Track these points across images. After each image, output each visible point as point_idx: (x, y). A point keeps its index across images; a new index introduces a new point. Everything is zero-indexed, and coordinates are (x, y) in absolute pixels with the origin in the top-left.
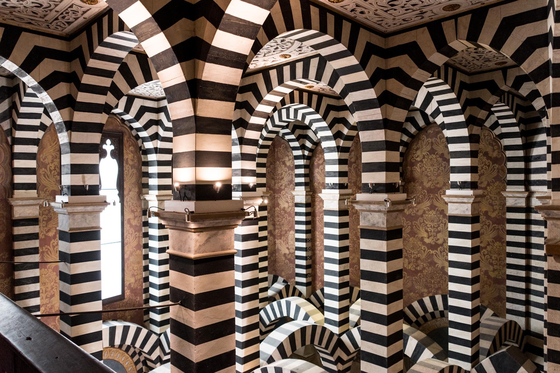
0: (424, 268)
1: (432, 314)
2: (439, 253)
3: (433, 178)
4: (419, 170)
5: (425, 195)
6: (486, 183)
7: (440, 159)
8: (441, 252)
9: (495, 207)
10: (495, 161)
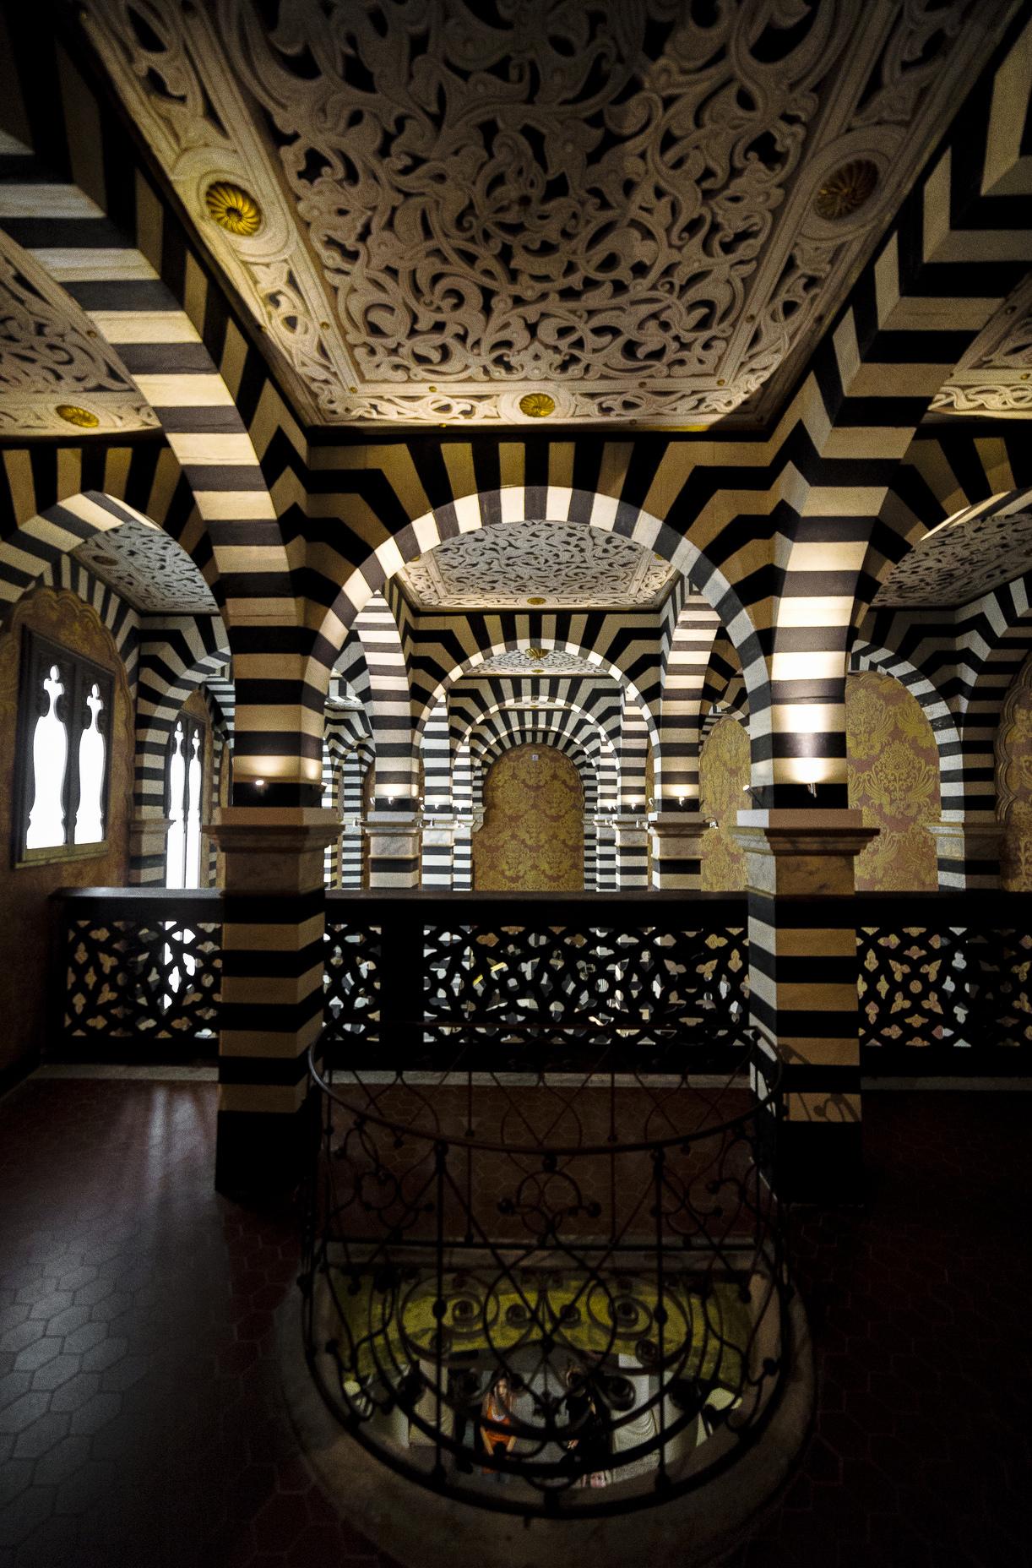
10: (572, 789)
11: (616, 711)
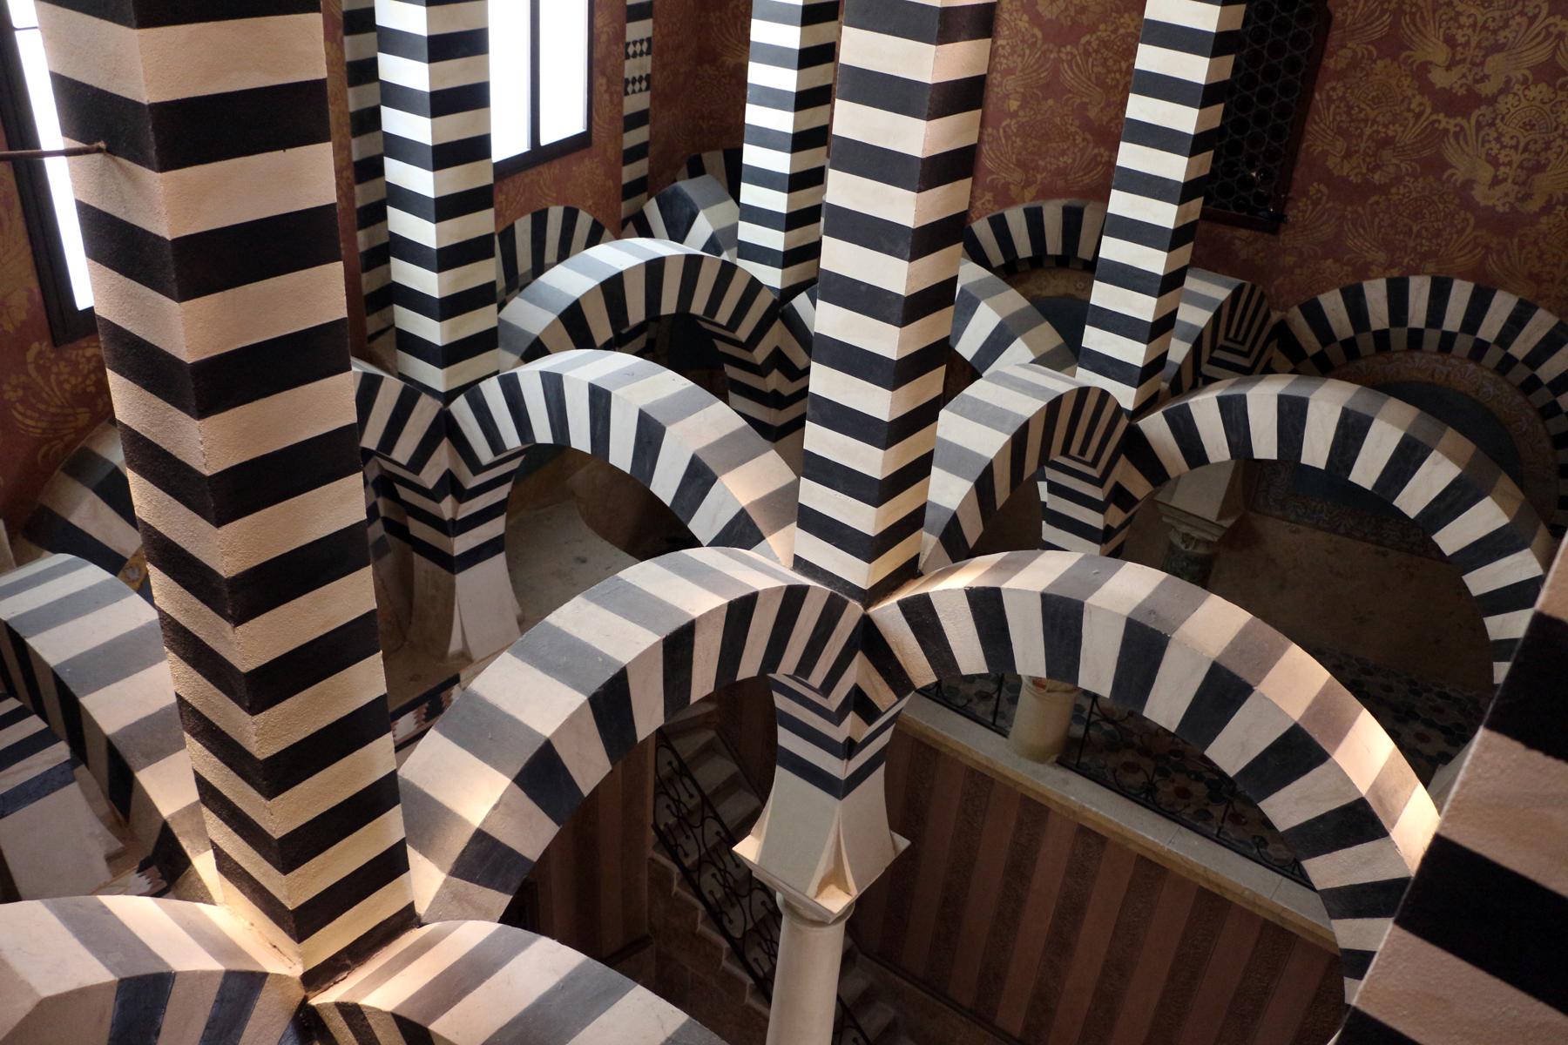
0: (1398, 180)
1: (1382, 338)
8: (1479, 126)
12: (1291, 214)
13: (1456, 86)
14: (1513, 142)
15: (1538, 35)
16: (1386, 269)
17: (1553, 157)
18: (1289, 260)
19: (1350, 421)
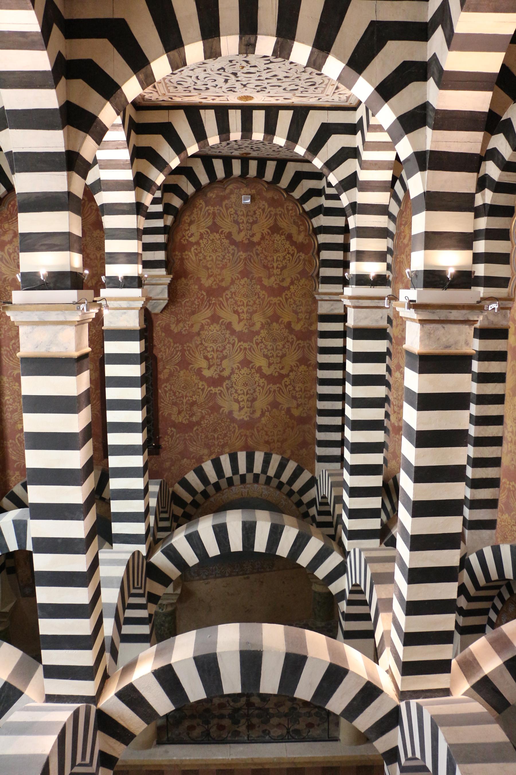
0: (203, 417)
1: (217, 486)
2: (225, 391)
3: (216, 271)
4: (194, 258)
5: (203, 300)
6: (288, 280)
7: (226, 242)
8: (228, 389)
9: (301, 316)
10: (301, 248)
11: (353, 153)
12: (163, 444)
13: (214, 375)
14: (242, 392)
15: (237, 350)
16: (210, 456)
17: (258, 394)
18: (168, 464)
19: (247, 526)
